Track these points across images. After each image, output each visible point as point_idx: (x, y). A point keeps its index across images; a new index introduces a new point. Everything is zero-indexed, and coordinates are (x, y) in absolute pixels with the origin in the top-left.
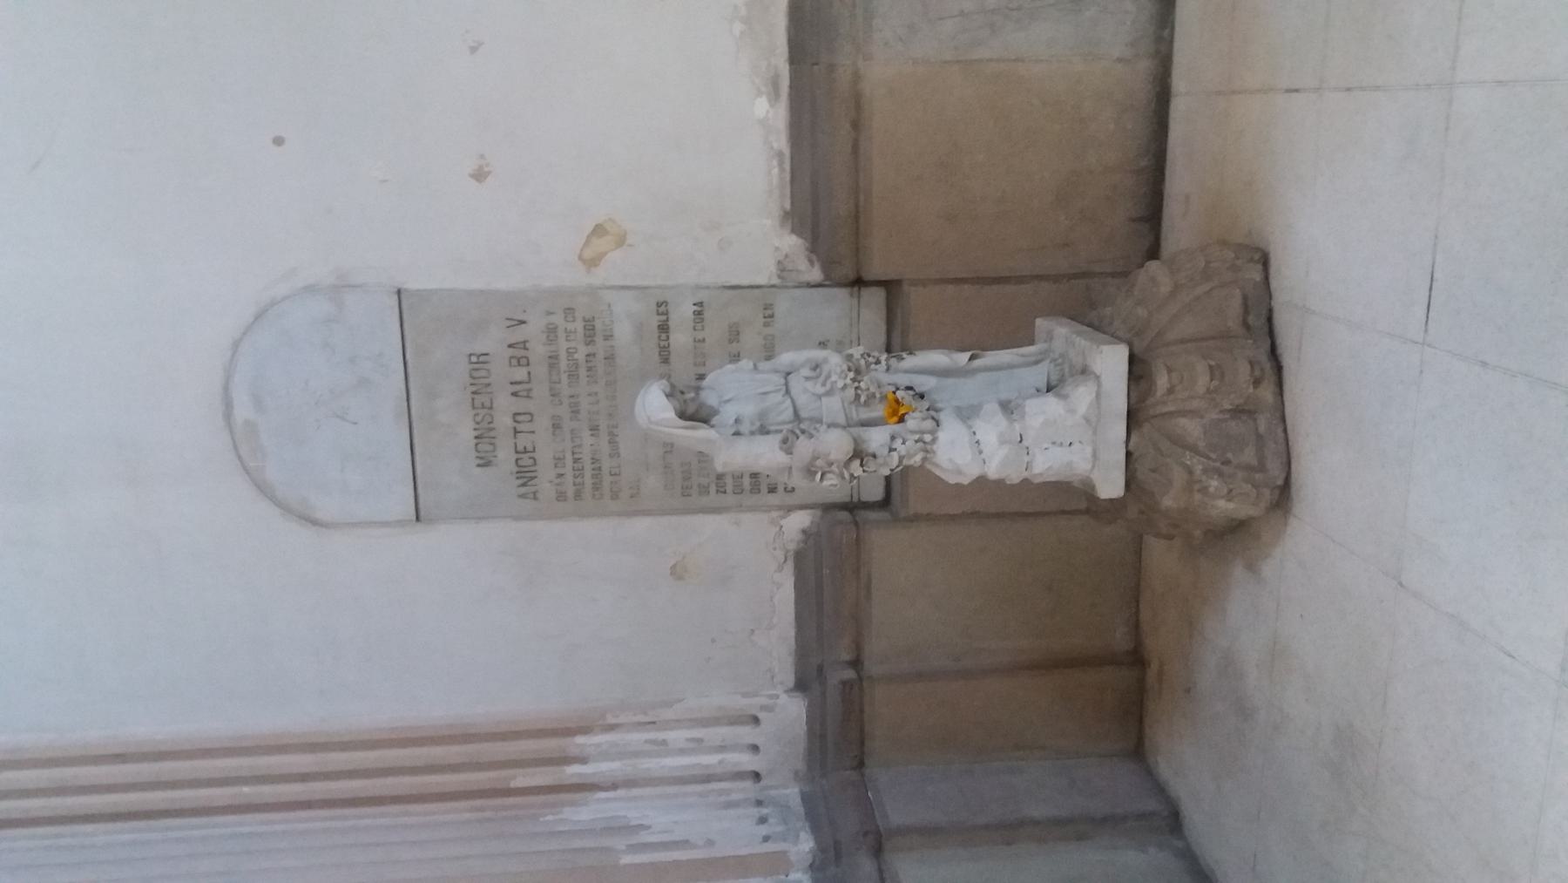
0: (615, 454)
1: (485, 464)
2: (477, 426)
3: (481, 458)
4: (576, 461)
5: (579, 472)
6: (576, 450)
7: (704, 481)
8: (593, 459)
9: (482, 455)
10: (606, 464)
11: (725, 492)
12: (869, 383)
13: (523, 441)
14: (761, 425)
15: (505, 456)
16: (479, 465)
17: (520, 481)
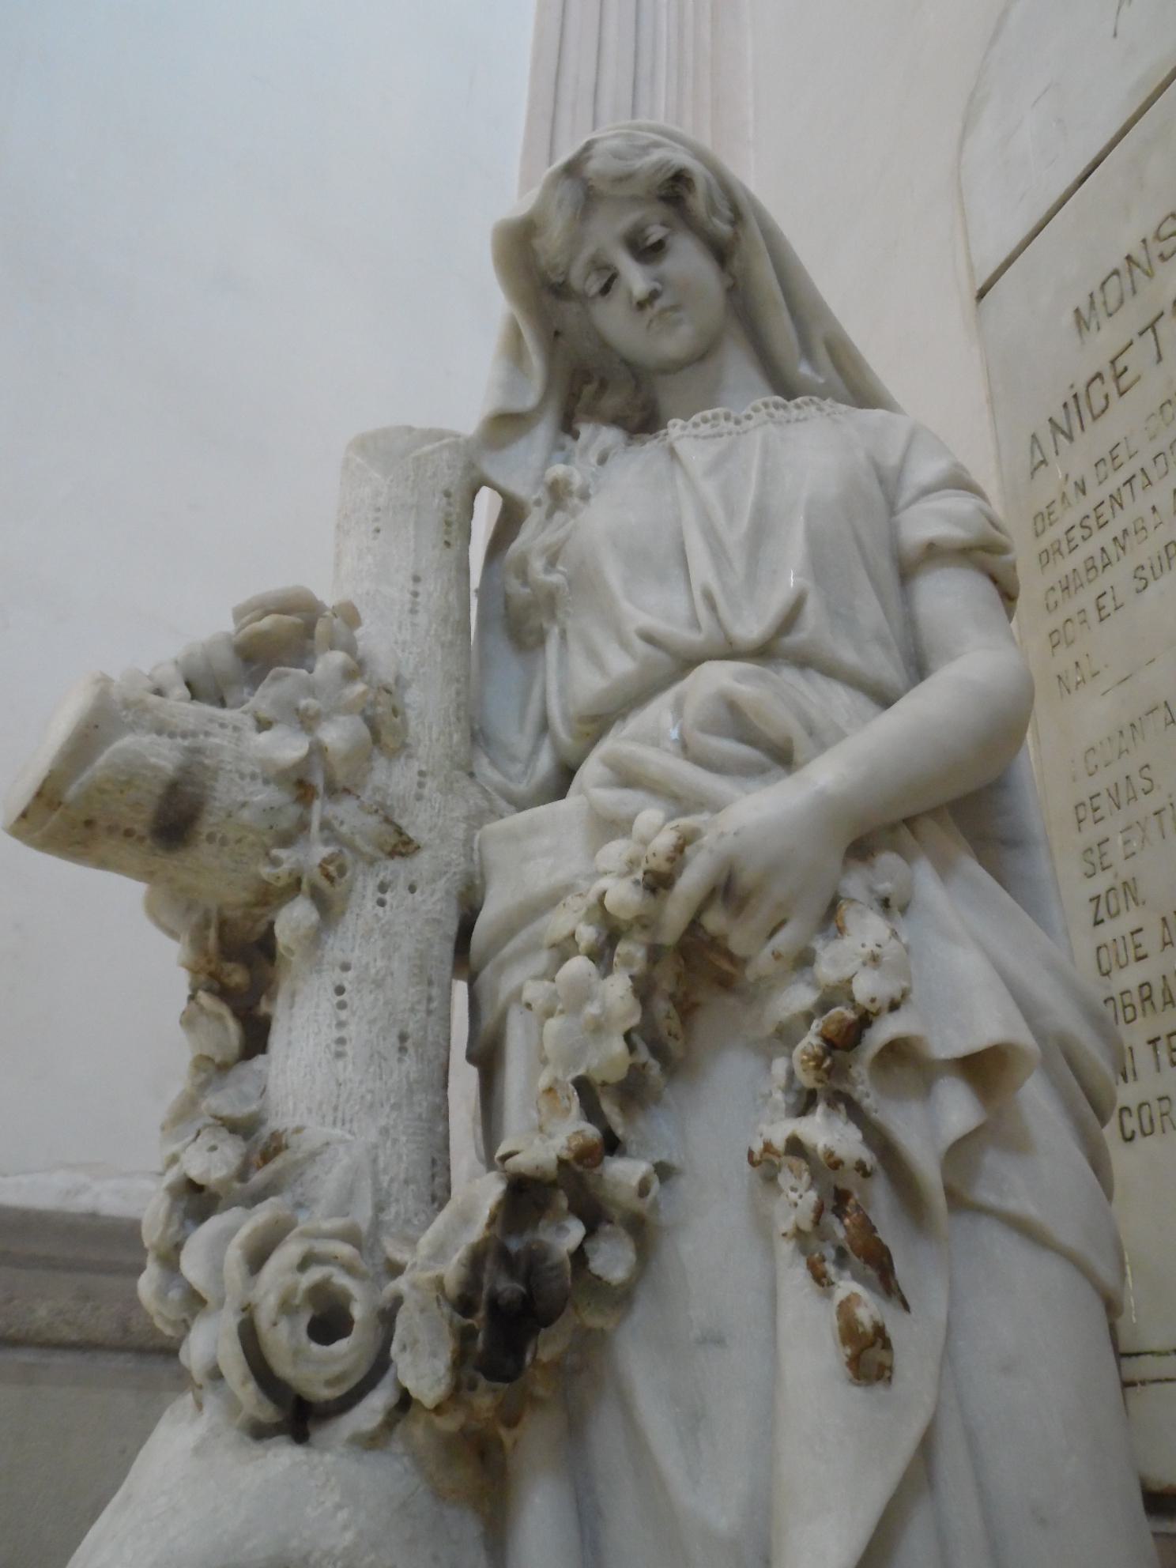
0: (1142, 579)
1: (1081, 322)
2: (1150, 238)
3: (1092, 304)
4: (1116, 500)
5: (1100, 520)
6: (1139, 482)
7: (1116, 851)
8: (1125, 532)
9: (1098, 299)
10: (1119, 576)
11: (1098, 923)
12: (592, 1009)
13: (1139, 359)
14: (550, 601)
15: (1107, 338)
16: (1077, 311)
17: (1061, 420)
